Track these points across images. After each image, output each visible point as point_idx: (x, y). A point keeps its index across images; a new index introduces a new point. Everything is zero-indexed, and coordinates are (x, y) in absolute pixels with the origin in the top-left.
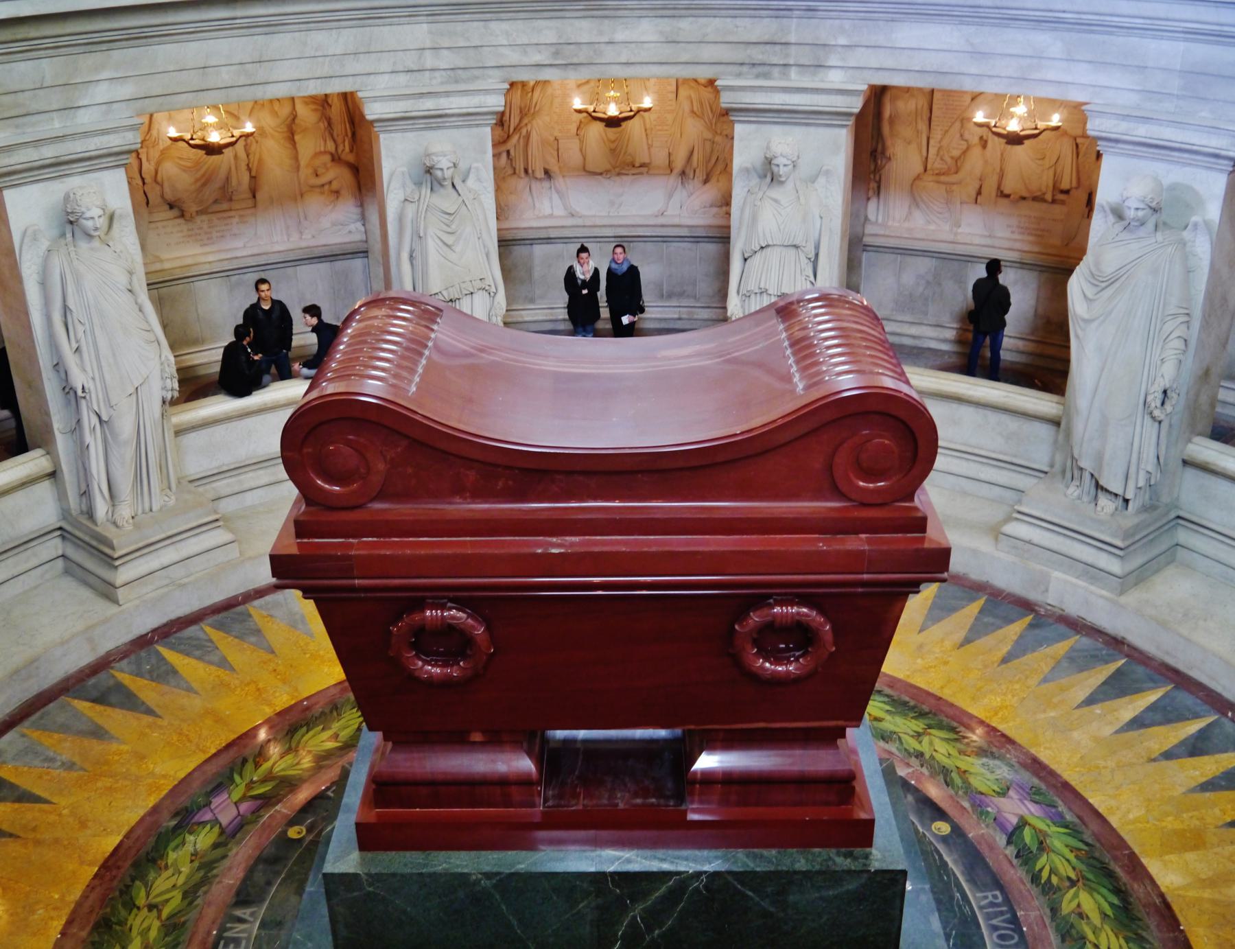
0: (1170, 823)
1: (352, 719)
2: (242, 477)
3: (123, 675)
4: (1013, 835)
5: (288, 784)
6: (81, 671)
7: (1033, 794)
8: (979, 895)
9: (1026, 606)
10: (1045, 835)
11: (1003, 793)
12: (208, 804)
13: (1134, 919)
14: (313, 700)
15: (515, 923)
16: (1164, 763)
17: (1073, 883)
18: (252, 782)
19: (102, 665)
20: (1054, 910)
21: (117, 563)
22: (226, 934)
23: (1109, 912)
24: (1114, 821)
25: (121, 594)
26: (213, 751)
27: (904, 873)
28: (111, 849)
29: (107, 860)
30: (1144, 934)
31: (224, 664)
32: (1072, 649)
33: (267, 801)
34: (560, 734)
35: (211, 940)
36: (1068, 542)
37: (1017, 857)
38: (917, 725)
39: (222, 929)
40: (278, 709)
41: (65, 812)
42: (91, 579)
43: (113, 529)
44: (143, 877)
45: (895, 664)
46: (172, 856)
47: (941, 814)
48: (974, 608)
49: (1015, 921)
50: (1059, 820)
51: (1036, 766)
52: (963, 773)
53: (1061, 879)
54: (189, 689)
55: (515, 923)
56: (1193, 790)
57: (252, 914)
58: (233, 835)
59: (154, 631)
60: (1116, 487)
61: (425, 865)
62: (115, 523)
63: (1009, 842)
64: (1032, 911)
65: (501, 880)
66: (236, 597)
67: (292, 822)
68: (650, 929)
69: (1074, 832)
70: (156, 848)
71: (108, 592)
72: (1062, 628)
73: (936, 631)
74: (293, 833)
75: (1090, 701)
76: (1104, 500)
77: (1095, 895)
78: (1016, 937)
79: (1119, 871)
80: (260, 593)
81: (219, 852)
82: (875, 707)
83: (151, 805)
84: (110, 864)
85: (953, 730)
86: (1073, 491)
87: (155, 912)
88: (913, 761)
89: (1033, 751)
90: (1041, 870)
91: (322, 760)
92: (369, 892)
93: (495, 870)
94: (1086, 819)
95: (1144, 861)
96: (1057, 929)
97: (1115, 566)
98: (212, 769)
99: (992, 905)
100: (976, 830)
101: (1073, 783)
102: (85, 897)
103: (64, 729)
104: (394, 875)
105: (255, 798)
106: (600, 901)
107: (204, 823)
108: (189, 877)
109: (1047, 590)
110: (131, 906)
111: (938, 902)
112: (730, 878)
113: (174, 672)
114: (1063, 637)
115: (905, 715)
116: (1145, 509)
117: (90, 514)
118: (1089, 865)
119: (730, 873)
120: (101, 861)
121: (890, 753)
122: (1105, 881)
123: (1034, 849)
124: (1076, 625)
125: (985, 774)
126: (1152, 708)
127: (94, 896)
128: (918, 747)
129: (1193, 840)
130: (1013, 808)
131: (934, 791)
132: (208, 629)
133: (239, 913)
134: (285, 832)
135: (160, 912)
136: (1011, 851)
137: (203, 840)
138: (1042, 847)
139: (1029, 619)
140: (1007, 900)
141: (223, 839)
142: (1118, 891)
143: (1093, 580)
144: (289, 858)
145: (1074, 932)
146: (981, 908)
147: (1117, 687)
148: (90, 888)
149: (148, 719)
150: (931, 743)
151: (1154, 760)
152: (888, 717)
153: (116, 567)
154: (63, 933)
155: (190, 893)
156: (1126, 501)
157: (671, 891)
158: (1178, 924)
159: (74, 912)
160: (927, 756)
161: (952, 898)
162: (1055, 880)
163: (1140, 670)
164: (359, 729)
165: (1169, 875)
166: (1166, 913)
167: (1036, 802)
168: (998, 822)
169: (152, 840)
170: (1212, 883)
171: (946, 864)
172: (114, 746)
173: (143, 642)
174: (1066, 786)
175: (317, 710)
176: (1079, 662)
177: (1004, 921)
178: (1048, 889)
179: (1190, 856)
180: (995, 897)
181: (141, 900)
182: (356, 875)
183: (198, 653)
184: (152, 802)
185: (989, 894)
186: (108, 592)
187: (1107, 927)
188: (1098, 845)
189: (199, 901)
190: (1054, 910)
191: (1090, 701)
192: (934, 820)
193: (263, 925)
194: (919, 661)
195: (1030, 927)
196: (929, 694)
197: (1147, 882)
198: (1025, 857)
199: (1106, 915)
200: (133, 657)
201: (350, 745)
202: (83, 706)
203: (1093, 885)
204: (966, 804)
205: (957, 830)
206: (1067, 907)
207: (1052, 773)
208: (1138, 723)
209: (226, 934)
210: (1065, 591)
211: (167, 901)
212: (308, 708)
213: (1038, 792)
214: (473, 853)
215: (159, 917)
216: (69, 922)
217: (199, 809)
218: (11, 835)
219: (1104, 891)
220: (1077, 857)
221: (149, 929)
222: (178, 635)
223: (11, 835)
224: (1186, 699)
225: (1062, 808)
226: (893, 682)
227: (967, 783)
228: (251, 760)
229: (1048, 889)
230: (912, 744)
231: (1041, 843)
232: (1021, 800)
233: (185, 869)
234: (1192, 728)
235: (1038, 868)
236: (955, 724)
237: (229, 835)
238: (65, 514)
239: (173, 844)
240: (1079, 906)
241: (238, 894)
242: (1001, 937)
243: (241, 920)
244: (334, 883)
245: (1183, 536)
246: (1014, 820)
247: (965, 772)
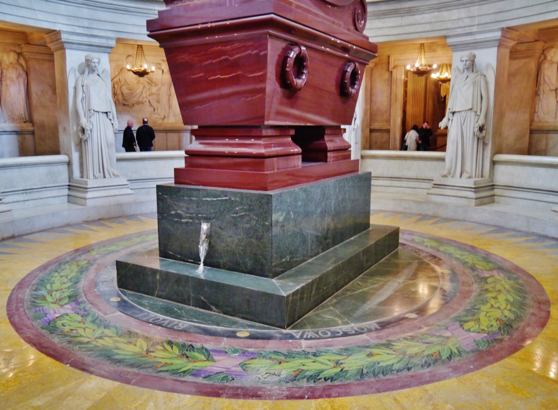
7: (227, 376)
13: (101, 355)
17: (148, 351)
23: (116, 351)
24: (161, 395)
30: (89, 353)
53: (157, 350)
77: (132, 354)
79: (130, 370)
90: (172, 347)
101: (215, 399)
118: (150, 363)
136: (198, 345)
142: (119, 361)
158: (72, 365)
174: (218, 395)
177: (163, 323)
188: (155, 375)
195: (150, 327)
197: (106, 374)
199: (117, 349)
203: (136, 356)
207: (236, 396)
220: (161, 362)
231: (187, 357)
232: (228, 368)
240: (135, 345)
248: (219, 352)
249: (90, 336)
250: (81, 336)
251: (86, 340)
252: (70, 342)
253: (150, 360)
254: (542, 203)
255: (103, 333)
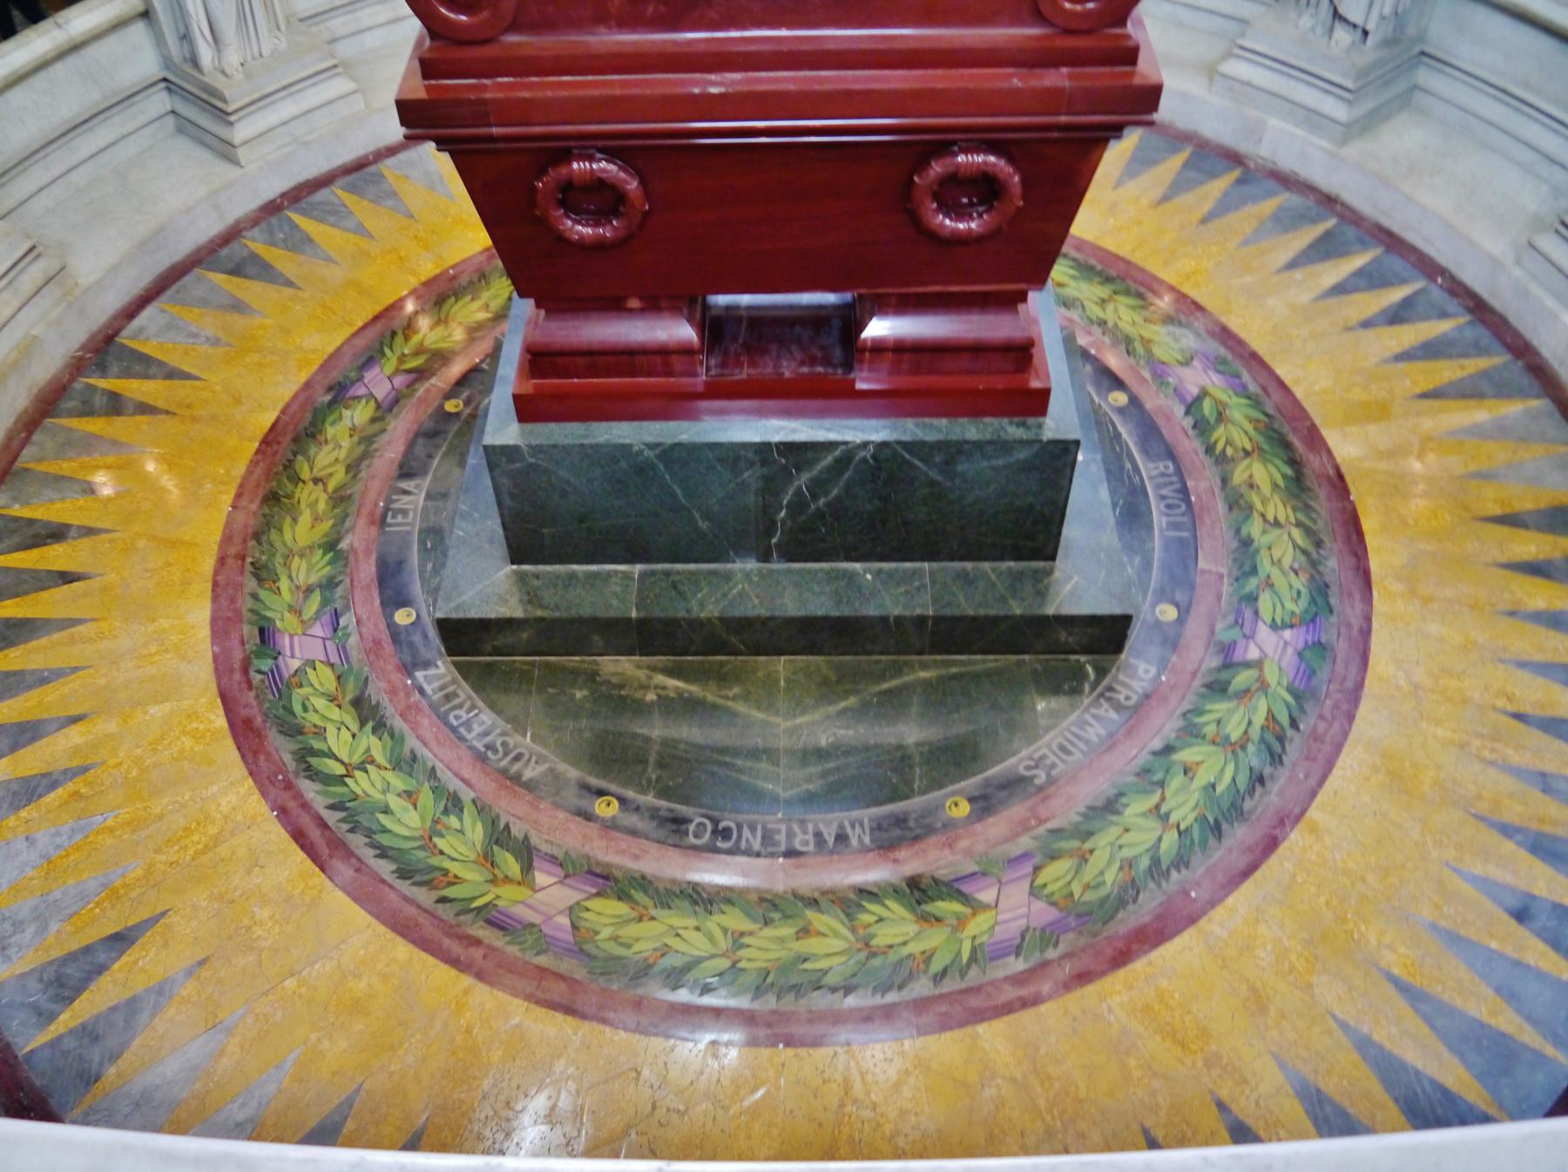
0: (1358, 395)
1: (502, 287)
2: (359, 14)
3: (255, 243)
4: (1192, 407)
5: (441, 357)
6: (211, 241)
7: (1218, 364)
8: (1151, 465)
9: (1234, 158)
10: (1225, 405)
11: (1187, 363)
12: (361, 379)
14: (459, 269)
15: (679, 492)
16: (1362, 333)
17: (1247, 454)
18: (404, 355)
19: (232, 234)
20: (1225, 481)
21: (232, 118)
22: (393, 506)
23: (1281, 482)
24: (1299, 392)
25: (241, 153)
26: (360, 324)
27: (1077, 443)
28: (269, 425)
29: (266, 436)
30: (1313, 504)
31: (361, 230)
32: (1280, 208)
33: (421, 374)
34: (721, 300)
35: (379, 511)
36: (1292, 83)
37: (1195, 427)
38: (1102, 291)
39: (389, 501)
40: (423, 279)
41: (218, 388)
42: (207, 138)
43: (223, 79)
44: (305, 453)
45: (1087, 224)
46: (330, 431)
47: (1118, 384)
48: (1176, 161)
49: (1184, 491)
50: (1242, 391)
51: (1226, 335)
52: (1146, 343)
53: (1236, 449)
54: (328, 259)
55: (679, 492)
56: (1386, 361)
57: (417, 487)
58: (390, 410)
59: (283, 195)
60: (1355, 15)
61: (586, 437)
62: (223, 72)
63: (1187, 413)
64: (1203, 482)
65: (664, 451)
66: (366, 156)
67: (449, 396)
68: (815, 497)
69: (1256, 402)
70: (313, 424)
71: (226, 151)
72: (1272, 184)
73: (1132, 187)
74: (450, 406)
75: (1292, 265)
76: (1343, 36)
77: (1270, 466)
78: (1184, 507)
80: (391, 151)
81: (377, 427)
82: (1060, 271)
83: (303, 380)
84: (269, 440)
85: (1140, 296)
86: (1306, 21)
87: (320, 485)
88: (1096, 330)
89: (1224, 319)
91: (474, 331)
92: (531, 465)
93: (659, 440)
94: (1271, 390)
95: (1325, 433)
96: (1226, 498)
97: (1339, 111)
98: (360, 342)
99: (1163, 475)
100: (1153, 401)
102: (249, 472)
103: (203, 303)
104: (555, 446)
105: (408, 371)
106: (765, 470)
107: (358, 398)
108: (351, 449)
109: (1260, 140)
110: (297, 480)
111: (1108, 472)
112: (899, 448)
113: (310, 240)
114: (1270, 194)
115: (1090, 280)
116: (1389, 43)
117: (194, 61)
119: (899, 443)
120: (260, 437)
121: (1070, 320)
122: (1281, 452)
123: (1212, 421)
124: (1286, 181)
125: (1169, 343)
126: (1360, 273)
127: (258, 471)
128: (1101, 315)
129: (1377, 412)
130: (1195, 379)
131: (1114, 361)
132: (339, 192)
133: (404, 485)
134: (441, 407)
135: (325, 485)
136: (1188, 422)
137: (359, 414)
138: (1221, 417)
139: (1237, 173)
140: (1179, 471)
141: (379, 414)
142: (1294, 462)
143: (1313, 127)
144: (448, 430)
145: (1242, 502)
146: (1151, 478)
147: (1324, 249)
148: (254, 463)
149: (289, 291)
150: (1116, 310)
151: (1349, 329)
152: (1072, 283)
153: (231, 124)
154: (234, 507)
155: (353, 467)
156: (1365, 33)
157: (838, 461)
159: (241, 486)
160: (1110, 324)
161: (1122, 468)
162: (1229, 451)
163: (1350, 232)
164: (510, 299)
165: (1346, 446)
166: (1339, 484)
167: (1219, 372)
168: (1178, 393)
169: (309, 415)
170: (1391, 454)
171: (1118, 435)
172: (258, 321)
173: (272, 208)
174: (1254, 356)
175: (464, 280)
176: (1285, 222)
178: (1222, 460)
179: (1372, 428)
180: (1167, 467)
181: (305, 474)
182: (516, 448)
183: (332, 219)
184: (302, 378)
185: (1161, 465)
186: (226, 151)
187: (1277, 498)
189: (363, 474)
190: (1225, 481)
191: (1292, 265)
192: (1110, 390)
193: (429, 496)
194: (1111, 221)
195: (1198, 497)
196: (1118, 258)
198: (1202, 427)
200: (264, 225)
201: (501, 316)
202: (219, 278)
204: (1147, 374)
205: (1134, 401)
206: (1239, 476)
207: (1240, 342)
208: (1340, 289)
209: (393, 506)
210: (1283, 143)
211: (331, 475)
212: (454, 278)
213: (1224, 362)
214: (635, 424)
215: (325, 490)
216: (239, 495)
217: (353, 383)
218: (167, 412)
219: (1279, 462)
220: (1256, 429)
221: (317, 501)
222: (309, 199)
223: (167, 412)
224: (1397, 264)
225: (1246, 377)
226: (1081, 245)
227: (1149, 352)
228: (400, 333)
229: (1222, 460)
230: (1095, 311)
233: (346, 443)
234: (1397, 295)
235: (1213, 439)
236: (1143, 290)
237: (386, 409)
238: (167, 62)
239: (330, 419)
241: (401, 466)
242: (1169, 507)
243: (406, 492)
244: (497, 457)
245: (1424, 76)
246: (1195, 391)
247: (1149, 341)
248: (1181, 398)
249: (1286, 537)
250: (1295, 546)
251: (1297, 534)
252: (1319, 544)
253: (1261, 439)
254: (81, 169)
255: (1264, 532)
